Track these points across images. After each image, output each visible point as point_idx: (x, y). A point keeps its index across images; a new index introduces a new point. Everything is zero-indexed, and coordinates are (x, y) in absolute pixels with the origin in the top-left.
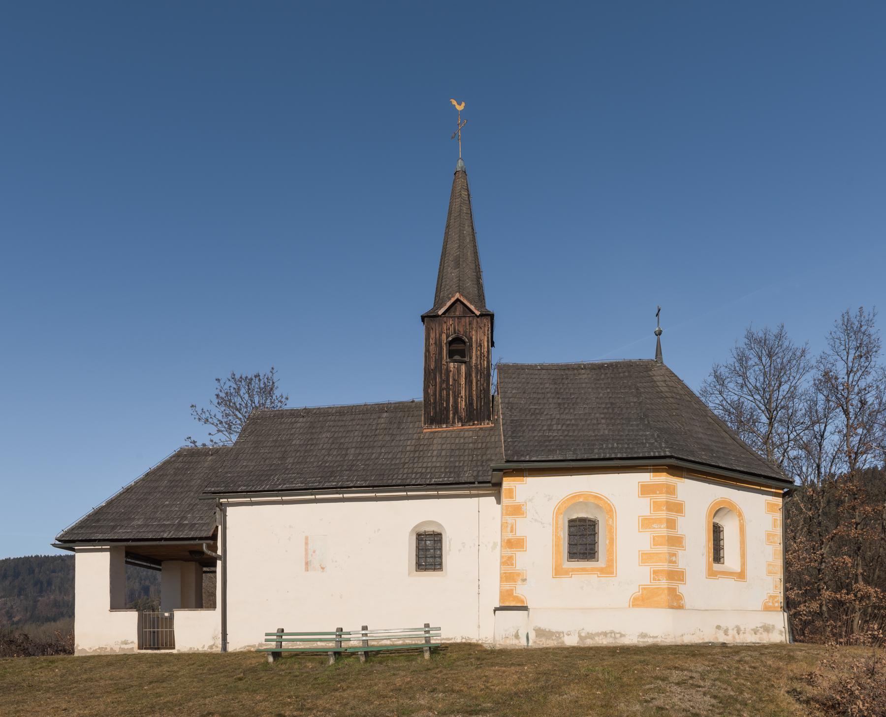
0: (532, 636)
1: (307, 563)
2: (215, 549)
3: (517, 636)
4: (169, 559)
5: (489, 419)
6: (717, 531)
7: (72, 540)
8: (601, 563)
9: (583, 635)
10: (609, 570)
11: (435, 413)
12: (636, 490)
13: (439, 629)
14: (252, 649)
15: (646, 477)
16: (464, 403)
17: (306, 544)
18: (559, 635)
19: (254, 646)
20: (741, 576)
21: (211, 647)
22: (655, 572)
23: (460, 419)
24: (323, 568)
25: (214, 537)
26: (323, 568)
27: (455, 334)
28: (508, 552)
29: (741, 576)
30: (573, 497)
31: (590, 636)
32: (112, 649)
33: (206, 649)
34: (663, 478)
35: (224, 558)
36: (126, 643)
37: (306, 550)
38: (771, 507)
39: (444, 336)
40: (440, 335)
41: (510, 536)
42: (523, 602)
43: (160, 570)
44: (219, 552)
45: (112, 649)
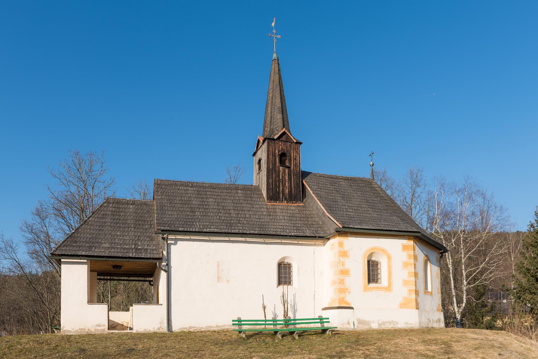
0: (356, 323)
1: (218, 278)
3: (349, 323)
5: (300, 201)
9: (380, 323)
11: (273, 194)
12: (400, 248)
13: (328, 319)
14: (185, 330)
15: (405, 242)
16: (287, 190)
17: (218, 266)
18: (368, 323)
19: (186, 328)
21: (159, 329)
22: (410, 290)
23: (286, 199)
24: (228, 281)
26: (228, 281)
27: (282, 152)
28: (342, 277)
30: (372, 249)
31: (383, 323)
32: (89, 330)
33: (156, 330)
36: (99, 325)
37: (218, 270)
39: (277, 151)
40: (275, 150)
41: (342, 268)
42: (349, 304)
45: (89, 330)
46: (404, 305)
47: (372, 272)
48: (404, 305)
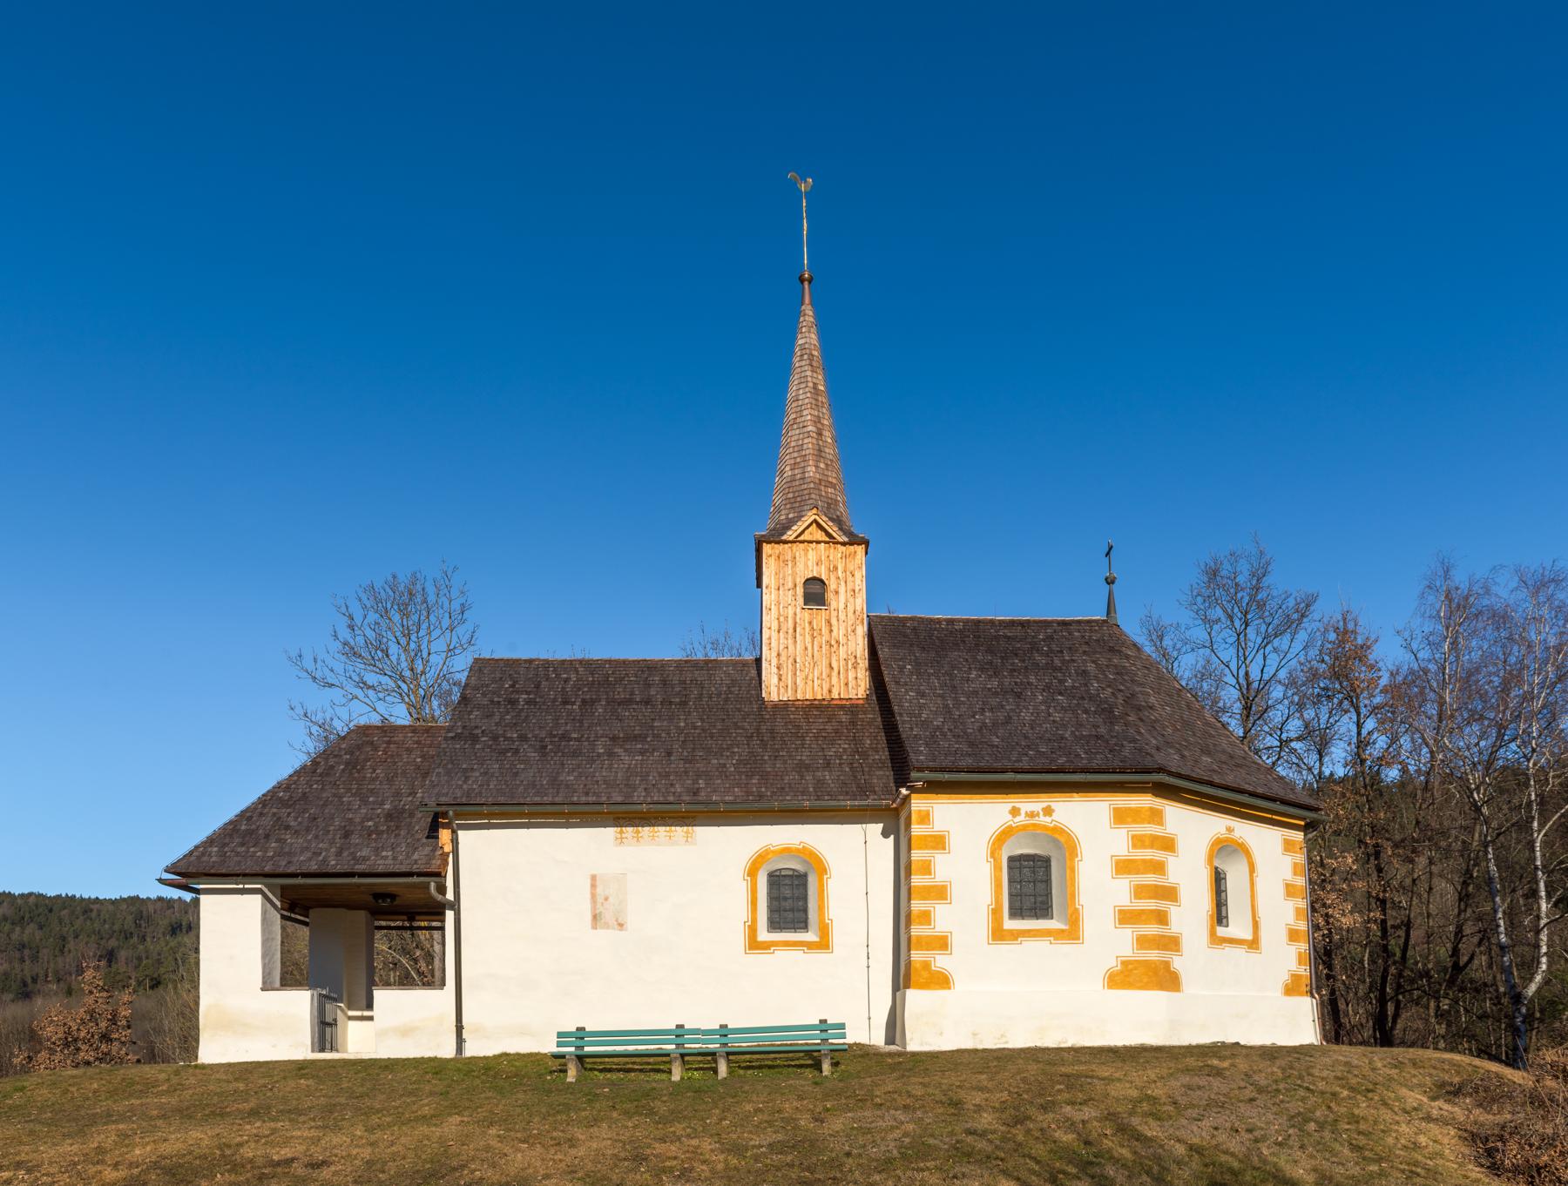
1: (595, 917)
2: (442, 889)
4: (361, 908)
6: (1219, 879)
7: (198, 871)
8: (1010, 924)
10: (1072, 933)
17: (593, 886)
20: (1253, 944)
24: (621, 925)
25: (439, 875)
26: (621, 925)
29: (1253, 944)
34: (1145, 801)
35: (455, 906)
37: (593, 896)
38: (1288, 846)
43: (306, 924)
44: (450, 896)
46: (1125, 977)
47: (1032, 887)
48: (1125, 977)
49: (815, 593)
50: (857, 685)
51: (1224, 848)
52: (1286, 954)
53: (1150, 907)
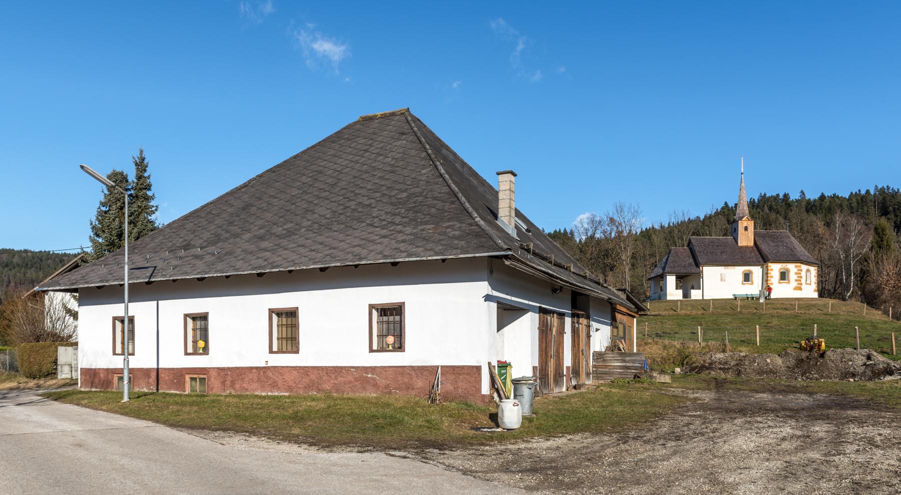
10: (789, 282)
47: (784, 276)
49: (746, 229)
50: (752, 244)
51: (808, 271)
52: (814, 286)
53: (798, 280)
